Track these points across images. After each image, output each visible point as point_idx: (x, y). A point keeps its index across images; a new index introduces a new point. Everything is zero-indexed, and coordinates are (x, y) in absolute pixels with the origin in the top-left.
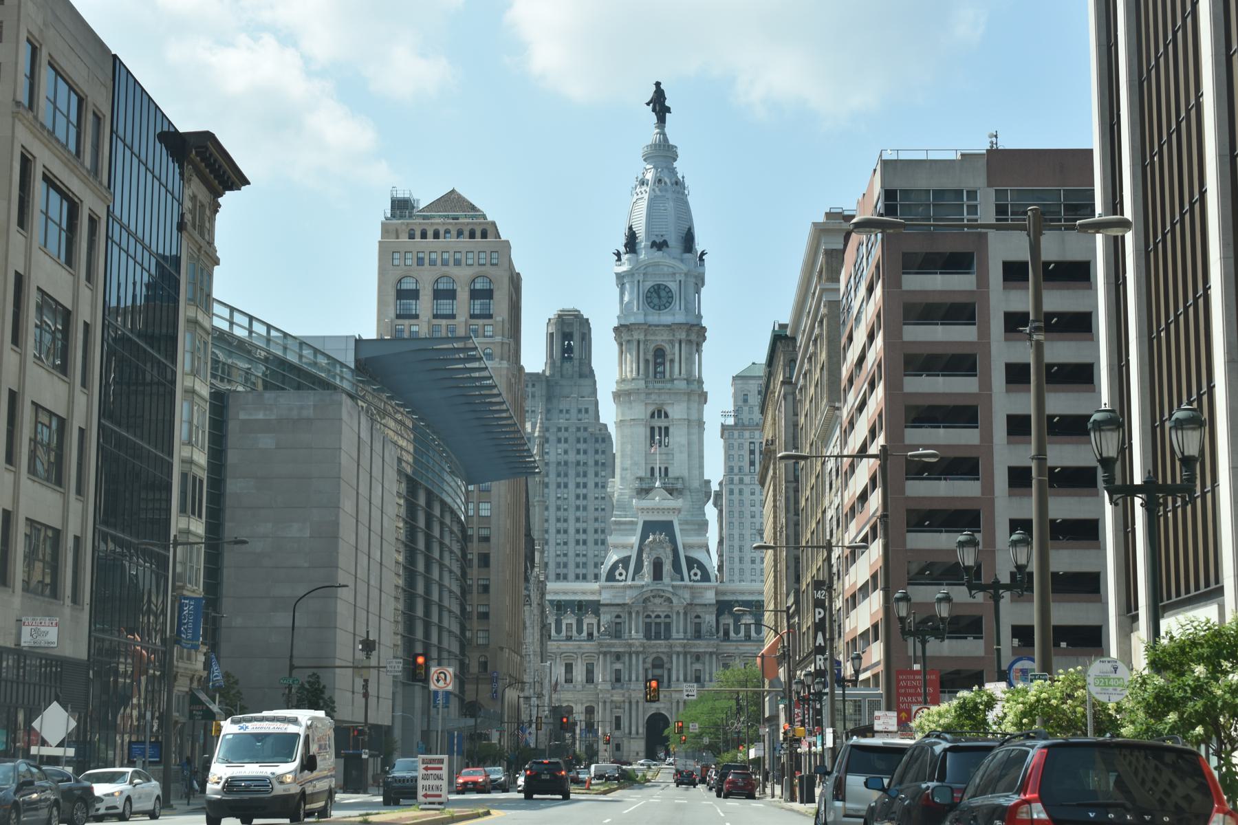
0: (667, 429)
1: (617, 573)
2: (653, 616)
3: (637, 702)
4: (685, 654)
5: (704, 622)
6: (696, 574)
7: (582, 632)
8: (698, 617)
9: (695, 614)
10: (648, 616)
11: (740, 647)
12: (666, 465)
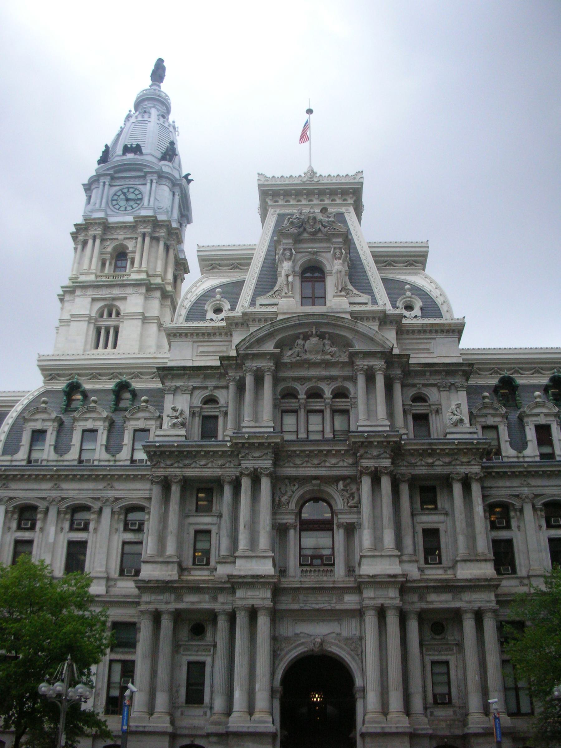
2: (302, 390)
3: (253, 613)
5: (437, 412)
7: (120, 450)
8: (419, 398)
9: (412, 392)
10: (291, 394)
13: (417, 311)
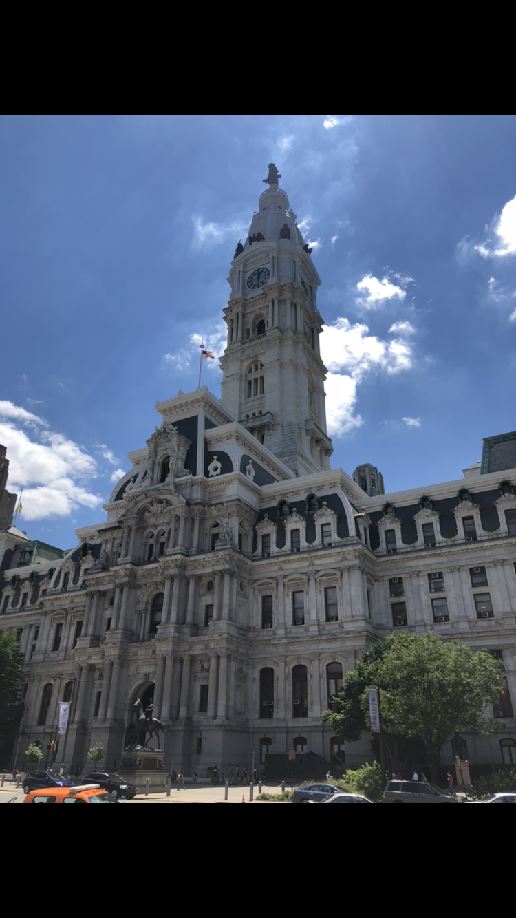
0: (262, 378)
1: (127, 489)
4: (185, 580)
6: (216, 469)
11: (285, 567)
12: (259, 409)
13: (219, 471)
